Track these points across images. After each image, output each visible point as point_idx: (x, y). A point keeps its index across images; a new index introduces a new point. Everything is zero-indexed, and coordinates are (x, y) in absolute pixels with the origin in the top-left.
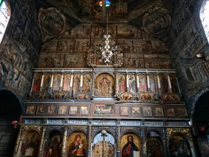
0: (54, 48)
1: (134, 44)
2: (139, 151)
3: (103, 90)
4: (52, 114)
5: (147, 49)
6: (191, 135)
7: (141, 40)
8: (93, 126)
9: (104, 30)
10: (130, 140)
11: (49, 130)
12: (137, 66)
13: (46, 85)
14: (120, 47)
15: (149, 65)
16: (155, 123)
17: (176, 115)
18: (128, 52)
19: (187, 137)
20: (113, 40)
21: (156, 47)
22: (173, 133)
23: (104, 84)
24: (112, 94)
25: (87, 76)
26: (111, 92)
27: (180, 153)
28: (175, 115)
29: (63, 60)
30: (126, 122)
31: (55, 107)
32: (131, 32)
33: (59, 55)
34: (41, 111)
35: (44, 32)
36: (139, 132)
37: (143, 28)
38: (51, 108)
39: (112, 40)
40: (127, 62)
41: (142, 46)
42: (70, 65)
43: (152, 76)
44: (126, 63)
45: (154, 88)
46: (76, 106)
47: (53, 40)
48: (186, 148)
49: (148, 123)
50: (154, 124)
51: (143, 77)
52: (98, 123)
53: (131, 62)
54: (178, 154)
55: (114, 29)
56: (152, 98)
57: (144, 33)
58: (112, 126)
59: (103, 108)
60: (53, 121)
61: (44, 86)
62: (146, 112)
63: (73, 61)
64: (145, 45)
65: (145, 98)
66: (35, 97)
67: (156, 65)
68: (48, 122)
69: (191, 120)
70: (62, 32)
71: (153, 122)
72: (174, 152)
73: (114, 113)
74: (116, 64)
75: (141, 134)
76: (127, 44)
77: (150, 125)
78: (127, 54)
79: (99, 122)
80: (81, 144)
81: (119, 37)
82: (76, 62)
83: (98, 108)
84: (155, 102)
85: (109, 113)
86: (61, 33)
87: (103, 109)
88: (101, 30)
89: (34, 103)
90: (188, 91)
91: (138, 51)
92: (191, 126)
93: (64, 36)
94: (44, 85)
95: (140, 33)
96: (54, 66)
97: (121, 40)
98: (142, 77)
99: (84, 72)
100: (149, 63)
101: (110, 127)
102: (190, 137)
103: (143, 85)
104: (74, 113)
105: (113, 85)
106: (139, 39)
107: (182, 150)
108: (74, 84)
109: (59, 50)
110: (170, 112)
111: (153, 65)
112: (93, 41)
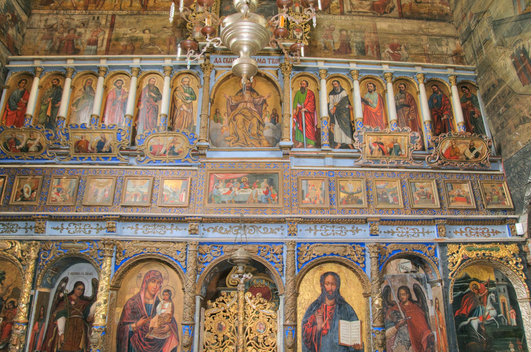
2: (359, 322)
3: (241, 127)
4: (62, 204)
6: (522, 263)
8: (201, 244)
10: (330, 286)
11: (54, 256)
15: (392, 52)
16: (412, 231)
17: (476, 204)
19: (510, 272)
22: (469, 258)
23: (245, 108)
24: (271, 142)
26: (267, 132)
27: (486, 323)
28: (473, 205)
29: (107, 32)
30: (319, 227)
31: (74, 180)
33: (94, 18)
34: (28, 192)
36: (359, 258)
38: (59, 184)
43: (403, 86)
46: (145, 178)
48: (504, 304)
49: (389, 232)
50: (407, 232)
51: (374, 86)
52: (220, 232)
53: (336, 40)
54: (479, 325)
56: (403, 151)
58: (271, 243)
59: (239, 185)
60: (66, 225)
62: (386, 194)
66: (6, 148)
67: (415, 54)
68: (51, 232)
69: (524, 218)
71: (406, 227)
72: (469, 319)
73: (278, 200)
75: (365, 267)
77: (396, 238)
79: (223, 231)
80: (162, 302)
82: (151, 39)
83: (221, 185)
84: (414, 164)
85: (260, 202)
87: (239, 189)
89: (5, 168)
90: (516, 127)
92: (522, 236)
94: (39, 111)
96: (77, 51)
98: (372, 85)
100: (394, 47)
101: (263, 245)
102: (518, 271)
104: (138, 200)
105: (275, 110)
107: (493, 313)
110: (459, 195)
111: (404, 53)
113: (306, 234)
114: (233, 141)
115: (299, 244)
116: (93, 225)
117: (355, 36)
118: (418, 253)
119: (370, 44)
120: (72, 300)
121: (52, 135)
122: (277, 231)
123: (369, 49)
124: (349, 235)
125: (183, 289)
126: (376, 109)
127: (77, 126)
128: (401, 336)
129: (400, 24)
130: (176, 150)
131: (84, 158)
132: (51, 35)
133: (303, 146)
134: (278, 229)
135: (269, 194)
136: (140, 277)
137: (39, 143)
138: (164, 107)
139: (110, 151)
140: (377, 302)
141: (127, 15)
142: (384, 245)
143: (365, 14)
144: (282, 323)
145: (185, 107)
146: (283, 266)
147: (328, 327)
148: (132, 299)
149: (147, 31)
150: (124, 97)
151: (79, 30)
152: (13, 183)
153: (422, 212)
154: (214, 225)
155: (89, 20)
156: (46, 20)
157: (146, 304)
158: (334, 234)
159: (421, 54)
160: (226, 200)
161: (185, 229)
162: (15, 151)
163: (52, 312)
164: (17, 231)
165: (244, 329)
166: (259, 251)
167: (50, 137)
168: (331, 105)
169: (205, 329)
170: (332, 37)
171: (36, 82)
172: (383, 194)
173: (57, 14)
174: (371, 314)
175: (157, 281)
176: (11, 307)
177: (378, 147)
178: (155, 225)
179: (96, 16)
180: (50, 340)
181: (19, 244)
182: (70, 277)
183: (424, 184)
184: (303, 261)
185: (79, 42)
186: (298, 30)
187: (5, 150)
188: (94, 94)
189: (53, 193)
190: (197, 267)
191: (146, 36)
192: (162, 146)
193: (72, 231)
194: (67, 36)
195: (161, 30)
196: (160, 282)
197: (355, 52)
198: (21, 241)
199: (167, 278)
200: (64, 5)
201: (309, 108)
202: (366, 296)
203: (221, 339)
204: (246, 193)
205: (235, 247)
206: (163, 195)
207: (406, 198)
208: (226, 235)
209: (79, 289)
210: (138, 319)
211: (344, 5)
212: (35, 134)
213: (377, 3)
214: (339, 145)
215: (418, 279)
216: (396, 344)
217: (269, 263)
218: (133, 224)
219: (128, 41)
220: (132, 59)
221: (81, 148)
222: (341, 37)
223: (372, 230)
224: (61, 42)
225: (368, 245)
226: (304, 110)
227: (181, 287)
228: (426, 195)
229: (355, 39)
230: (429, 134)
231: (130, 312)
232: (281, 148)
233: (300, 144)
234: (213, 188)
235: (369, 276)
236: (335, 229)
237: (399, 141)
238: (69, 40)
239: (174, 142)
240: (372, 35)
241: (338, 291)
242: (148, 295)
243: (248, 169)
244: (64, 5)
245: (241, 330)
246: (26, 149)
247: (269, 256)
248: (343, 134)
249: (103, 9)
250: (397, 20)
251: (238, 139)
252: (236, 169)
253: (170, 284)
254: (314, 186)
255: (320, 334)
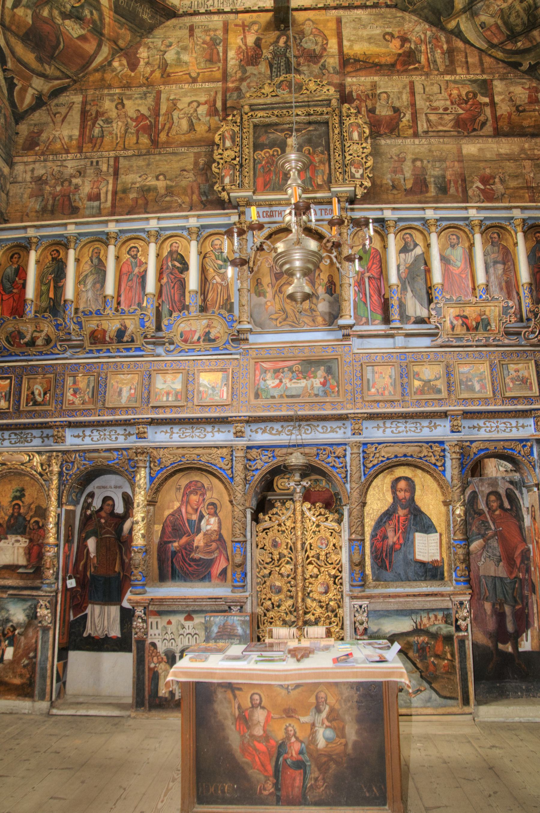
0: (69, 131)
1: (418, 97)
2: (438, 534)
4: (81, 407)
5: (473, 120)
7: (448, 77)
8: (249, 448)
9: (283, 40)
11: (78, 468)
12: (433, 194)
13: (48, 290)
14: (359, 112)
15: (482, 187)
16: (503, 425)
18: (392, 131)
20: (325, 82)
21: (514, 109)
24: (327, 318)
25: (217, 242)
30: (388, 424)
31: (92, 378)
32: (402, 46)
33: (92, 162)
35: (19, 61)
36: (437, 460)
37: (458, 24)
38: (75, 383)
39: (321, 82)
40: (387, 179)
41: (452, 103)
42: (140, 202)
43: (495, 235)
44: (384, 182)
45: (504, 284)
46: (177, 371)
47: (63, 99)
49: (474, 427)
50: (497, 427)
51: (458, 238)
53: (408, 174)
55: (326, 32)
56: (493, 325)
57: (460, 44)
58: (331, 445)
59: (290, 375)
60: (88, 432)
61: (41, 296)
62: (471, 381)
63: (154, 182)
64: (466, 102)
65: (464, 324)
66: (9, 343)
68: (72, 440)
70: (99, 59)
71: (495, 421)
73: (338, 391)
74: (340, 186)
76: (388, 96)
77: (483, 434)
78: (388, 141)
79: (274, 432)
80: (207, 517)
81: (349, 69)
82: (168, 188)
83: (269, 375)
84: (506, 341)
85: (316, 395)
86: (94, 65)
87: (291, 380)
88: (272, 41)
89: (9, 367)
91: (434, 129)
93: (108, 76)
94: (40, 294)
95: (441, 48)
96: (74, 211)
97: (357, 82)
98: (454, 237)
99: (204, 227)
100: (485, 180)
101: (322, 447)
103: (456, 271)
104: (170, 399)
106: (442, 74)
108: (165, 280)
109: (88, 140)
111: (499, 187)
112: (238, 89)
113: (374, 432)
114: (280, 319)
115: (365, 444)
116: (120, 430)
117: (434, 167)
118: (510, 452)
119: (453, 178)
120: (101, 517)
121: (61, 325)
122: (338, 430)
123: (452, 185)
124: (425, 431)
125: (231, 502)
126: (460, 270)
127: (91, 313)
128: (490, 550)
129: (494, 146)
130: (212, 336)
131: (101, 350)
132: (41, 190)
133: (367, 323)
134: (340, 428)
135: (328, 384)
136: (180, 489)
137: (47, 335)
138: (193, 281)
139: (132, 341)
140: (458, 512)
141: (134, 155)
142: (468, 444)
143: (446, 134)
144: (347, 538)
145: (218, 279)
146: (347, 471)
147: (402, 541)
148: (172, 515)
149: (161, 177)
150: (142, 270)
151: (74, 181)
152: (21, 385)
153: (516, 402)
154: (262, 425)
155: (86, 166)
156: (33, 170)
157: (188, 520)
158: (407, 432)
159: (522, 188)
160: (275, 394)
161: (229, 431)
162: (19, 345)
163: (80, 532)
164: (31, 440)
165: (303, 544)
166: (318, 454)
167: (60, 327)
168: (402, 268)
169: (257, 546)
170: (402, 171)
171: (33, 256)
172: (467, 381)
173: (45, 161)
174: (452, 526)
175: (199, 493)
176: (36, 527)
177: (460, 322)
178: (192, 428)
179: (94, 160)
180: (82, 563)
181: (37, 456)
182: (96, 491)
183: (520, 366)
184: (370, 465)
185: (77, 197)
186: (356, 165)
187: (7, 346)
188: (105, 267)
189: (69, 394)
190: (246, 476)
191: (161, 184)
192: (195, 331)
193: (95, 439)
194: (61, 191)
195: (180, 175)
196: (203, 494)
197: (432, 190)
198: (39, 453)
199: (211, 489)
200: (51, 147)
201: (375, 272)
202: (446, 504)
203: (276, 557)
204: (299, 385)
205: (290, 450)
206: (199, 392)
207: (496, 384)
208: (277, 437)
209: (109, 505)
210: (181, 538)
211: (419, 123)
212: (41, 325)
213: (463, 116)
214: (413, 319)
215: (511, 482)
216: (483, 560)
217: (330, 468)
218: (167, 428)
219: (138, 193)
220: (147, 219)
221: (97, 338)
222: (414, 170)
223: (453, 426)
224: (54, 199)
225: (448, 444)
226: (367, 275)
227: (227, 498)
228: (522, 380)
229: (433, 172)
230: (528, 301)
231: (170, 529)
232: (341, 327)
233: (364, 320)
234: (259, 380)
235: (450, 480)
236: (408, 425)
237: (487, 313)
238: (63, 196)
239: (208, 326)
240: (456, 164)
241: (412, 499)
242: (190, 510)
243: (301, 354)
244: (51, 147)
245: (299, 546)
246: (32, 343)
247: (329, 460)
248: (418, 306)
249: (102, 149)
250: (490, 140)
251: (287, 317)
252: (285, 355)
253: (214, 496)
254: (381, 373)
255: (392, 549)
